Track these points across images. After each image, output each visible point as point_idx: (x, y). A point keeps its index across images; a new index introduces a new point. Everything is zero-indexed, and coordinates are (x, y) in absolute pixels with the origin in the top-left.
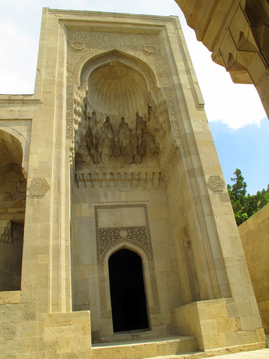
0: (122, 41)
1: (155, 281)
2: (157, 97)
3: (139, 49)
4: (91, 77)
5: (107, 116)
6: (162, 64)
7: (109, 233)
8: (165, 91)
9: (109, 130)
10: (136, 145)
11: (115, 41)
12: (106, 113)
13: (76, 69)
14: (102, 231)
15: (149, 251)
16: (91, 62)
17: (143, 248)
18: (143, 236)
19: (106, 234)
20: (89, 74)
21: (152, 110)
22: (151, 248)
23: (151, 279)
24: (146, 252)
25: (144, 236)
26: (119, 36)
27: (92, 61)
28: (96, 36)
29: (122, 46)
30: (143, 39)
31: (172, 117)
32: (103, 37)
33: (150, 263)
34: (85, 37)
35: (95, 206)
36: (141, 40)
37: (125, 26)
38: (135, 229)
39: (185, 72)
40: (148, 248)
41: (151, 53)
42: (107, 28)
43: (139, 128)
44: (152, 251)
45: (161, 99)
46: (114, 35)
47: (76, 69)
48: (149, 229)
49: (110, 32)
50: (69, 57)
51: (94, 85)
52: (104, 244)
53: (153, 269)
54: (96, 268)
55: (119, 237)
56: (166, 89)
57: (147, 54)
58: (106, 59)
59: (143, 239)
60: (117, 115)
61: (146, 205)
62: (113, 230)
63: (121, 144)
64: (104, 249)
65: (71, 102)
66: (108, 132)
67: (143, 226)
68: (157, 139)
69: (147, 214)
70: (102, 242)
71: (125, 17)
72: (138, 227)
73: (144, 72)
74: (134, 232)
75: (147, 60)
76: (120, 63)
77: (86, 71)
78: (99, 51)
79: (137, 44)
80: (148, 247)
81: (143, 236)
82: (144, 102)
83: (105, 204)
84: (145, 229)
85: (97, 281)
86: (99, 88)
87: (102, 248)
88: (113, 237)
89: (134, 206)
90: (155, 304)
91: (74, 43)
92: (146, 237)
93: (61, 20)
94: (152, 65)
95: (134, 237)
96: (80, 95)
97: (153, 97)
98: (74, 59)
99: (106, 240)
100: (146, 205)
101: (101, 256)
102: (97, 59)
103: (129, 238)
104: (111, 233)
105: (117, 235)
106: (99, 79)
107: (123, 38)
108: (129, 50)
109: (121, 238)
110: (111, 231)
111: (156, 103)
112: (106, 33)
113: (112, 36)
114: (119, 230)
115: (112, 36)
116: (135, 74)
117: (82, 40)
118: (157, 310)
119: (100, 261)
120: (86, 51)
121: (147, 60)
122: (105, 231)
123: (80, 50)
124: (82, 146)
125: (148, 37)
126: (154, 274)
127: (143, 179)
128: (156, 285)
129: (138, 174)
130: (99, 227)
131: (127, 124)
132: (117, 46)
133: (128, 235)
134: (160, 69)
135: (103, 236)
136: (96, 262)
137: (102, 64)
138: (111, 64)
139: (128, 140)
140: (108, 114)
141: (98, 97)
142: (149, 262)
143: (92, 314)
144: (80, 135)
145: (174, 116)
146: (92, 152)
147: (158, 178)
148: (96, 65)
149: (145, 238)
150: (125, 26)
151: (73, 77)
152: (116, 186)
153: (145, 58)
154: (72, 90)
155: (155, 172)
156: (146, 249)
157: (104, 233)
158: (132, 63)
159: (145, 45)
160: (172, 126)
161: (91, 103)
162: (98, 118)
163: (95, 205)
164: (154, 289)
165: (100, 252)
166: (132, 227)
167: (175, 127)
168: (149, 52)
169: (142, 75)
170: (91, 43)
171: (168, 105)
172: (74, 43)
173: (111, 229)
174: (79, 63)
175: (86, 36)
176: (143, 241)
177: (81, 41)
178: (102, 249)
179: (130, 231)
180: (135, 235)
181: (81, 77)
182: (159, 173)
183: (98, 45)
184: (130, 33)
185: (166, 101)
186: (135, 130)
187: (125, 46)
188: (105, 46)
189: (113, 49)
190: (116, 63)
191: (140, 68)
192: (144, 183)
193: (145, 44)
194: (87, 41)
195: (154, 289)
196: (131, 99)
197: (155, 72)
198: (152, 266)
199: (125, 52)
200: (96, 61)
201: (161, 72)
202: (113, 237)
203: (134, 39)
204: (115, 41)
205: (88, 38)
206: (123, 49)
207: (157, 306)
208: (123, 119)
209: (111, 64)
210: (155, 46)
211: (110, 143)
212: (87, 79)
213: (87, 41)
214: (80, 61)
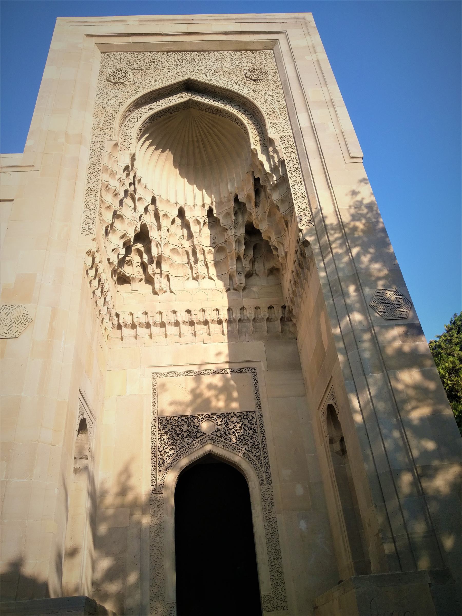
1: (275, 530)
2: (269, 158)
3: (234, 76)
6: (279, 96)
8: (283, 142)
11: (189, 65)
13: (111, 115)
15: (261, 463)
17: (249, 458)
18: (248, 431)
19: (173, 428)
22: (266, 457)
23: (267, 527)
24: (255, 465)
25: (251, 432)
26: (197, 57)
31: (296, 187)
33: (264, 490)
36: (240, 59)
38: (232, 417)
40: (259, 458)
41: (257, 80)
44: (267, 463)
47: (111, 115)
48: (262, 416)
50: (100, 96)
52: (167, 450)
53: (271, 504)
55: (199, 435)
56: (286, 139)
59: (249, 438)
61: (255, 368)
62: (185, 420)
64: (166, 460)
65: (96, 170)
67: (250, 412)
70: (164, 445)
72: (238, 413)
74: (230, 423)
75: (249, 92)
78: (157, 83)
80: (258, 454)
81: (248, 431)
84: (253, 417)
88: (185, 435)
90: (275, 586)
91: (111, 72)
92: (255, 432)
94: (258, 100)
95: (229, 433)
98: (109, 98)
99: (171, 442)
103: (219, 435)
105: (195, 430)
107: (204, 60)
108: (215, 79)
109: (202, 435)
110: (183, 423)
111: (267, 168)
113: (184, 58)
114: (199, 421)
118: (279, 603)
120: (134, 84)
122: (170, 421)
123: (122, 83)
125: (253, 55)
126: (273, 515)
128: (277, 541)
133: (218, 430)
142: (262, 487)
145: (299, 185)
149: (254, 436)
153: (246, 89)
156: (254, 458)
157: (168, 426)
160: (296, 204)
164: (273, 551)
166: (227, 413)
167: (300, 205)
168: (253, 78)
171: (289, 167)
173: (182, 418)
174: (118, 104)
175: (135, 61)
176: (248, 443)
178: (161, 461)
179: (221, 421)
180: (233, 430)
182: (282, 307)
183: (156, 74)
185: (284, 160)
193: (247, 66)
195: (273, 551)
198: (268, 496)
199: (207, 82)
202: (185, 435)
204: (189, 65)
206: (204, 77)
207: (280, 590)
214: (120, 101)
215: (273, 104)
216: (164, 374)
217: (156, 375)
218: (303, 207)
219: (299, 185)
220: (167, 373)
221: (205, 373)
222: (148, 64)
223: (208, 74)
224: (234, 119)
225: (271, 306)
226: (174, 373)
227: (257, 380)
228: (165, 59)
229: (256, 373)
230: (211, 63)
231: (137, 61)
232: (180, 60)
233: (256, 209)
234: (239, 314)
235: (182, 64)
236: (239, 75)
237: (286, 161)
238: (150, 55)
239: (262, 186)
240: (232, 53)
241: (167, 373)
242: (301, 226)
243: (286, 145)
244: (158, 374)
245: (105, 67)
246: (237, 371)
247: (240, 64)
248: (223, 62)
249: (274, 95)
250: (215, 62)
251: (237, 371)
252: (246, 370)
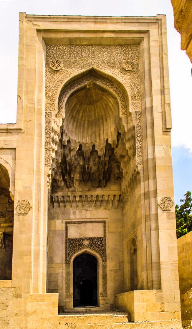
0: (101, 56)
2: (127, 123)
3: (116, 67)
4: (68, 103)
7: (75, 242)
9: (81, 157)
10: (103, 170)
11: (93, 57)
14: (70, 240)
16: (68, 85)
20: (66, 99)
21: (121, 137)
27: (69, 84)
28: (74, 51)
29: (100, 63)
30: (123, 53)
32: (82, 52)
34: (63, 53)
36: (121, 53)
37: (106, 35)
39: (159, 92)
42: (87, 39)
43: (107, 155)
45: (131, 124)
46: (93, 49)
49: (89, 45)
54: (64, 266)
57: (124, 72)
58: (83, 81)
60: (89, 142)
63: (91, 170)
66: (80, 159)
68: (122, 166)
71: (106, 22)
73: (119, 95)
76: (96, 85)
77: (64, 96)
79: (116, 60)
82: (115, 128)
85: (64, 275)
87: (69, 253)
89: (96, 222)
93: (39, 31)
94: (127, 86)
96: (57, 123)
97: (124, 123)
101: (68, 258)
102: (74, 81)
104: (77, 242)
107: (101, 53)
112: (85, 47)
115: (90, 51)
116: (109, 97)
117: (60, 58)
119: (67, 261)
121: (123, 79)
125: (128, 50)
127: (105, 201)
130: (68, 237)
132: (95, 64)
134: (135, 90)
135: (71, 244)
136: (64, 262)
137: (79, 86)
138: (88, 87)
139: (97, 167)
141: (73, 125)
143: (59, 296)
148: (73, 88)
150: (106, 35)
151: (51, 103)
152: (83, 206)
154: (50, 117)
158: (108, 84)
159: (123, 61)
162: (72, 145)
165: (68, 255)
169: (116, 98)
170: (68, 60)
172: (52, 62)
177: (59, 59)
181: (58, 104)
184: (109, 46)
186: (103, 157)
187: (103, 63)
188: (83, 64)
189: (91, 68)
191: (115, 90)
192: (106, 203)
193: (124, 59)
194: (65, 59)
196: (103, 125)
197: (129, 93)
200: (73, 84)
201: (135, 94)
203: (113, 53)
205: (66, 54)
206: (101, 67)
209: (88, 87)
210: (134, 61)
211: (81, 170)
212: (64, 106)
213: (65, 59)
215: (134, 89)
218: (140, 155)
219: (140, 142)
222: (71, 56)
223: (103, 65)
224: (113, 96)
228: (80, 51)
230: (105, 55)
231: (66, 52)
232: (89, 53)
235: (89, 56)
236: (119, 66)
237: (136, 127)
238: (73, 47)
240: (117, 48)
243: (137, 118)
245: (48, 57)
247: (120, 57)
248: (111, 55)
249: (135, 82)
250: (107, 55)
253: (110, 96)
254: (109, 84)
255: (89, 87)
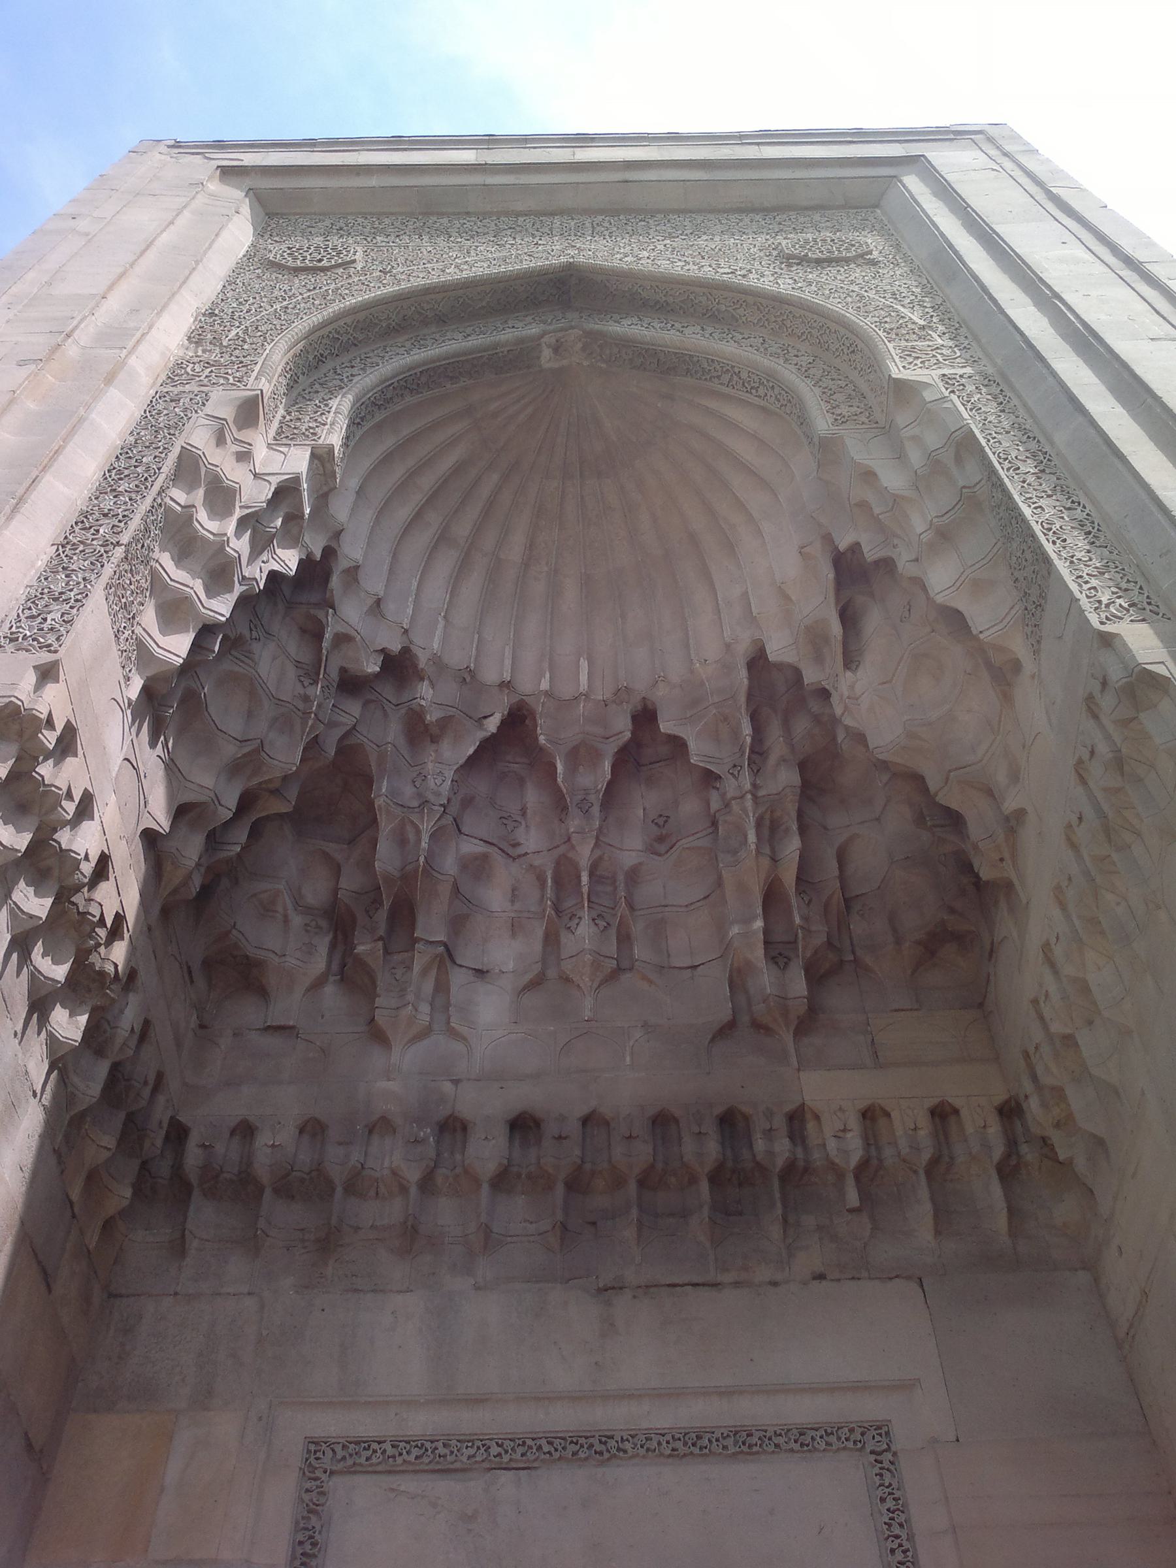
5: (515, 699)
12: (507, 677)
35: (315, 1447)
51: (415, 499)
61: (882, 1429)
69: (911, 1538)
83: (420, 1423)
86: (462, 530)
100: (882, 1429)
106: (458, 470)
124: (280, 909)
129: (779, 1122)
131: (678, 745)
138: (547, 358)
140: (526, 685)
144: (235, 768)
146: (360, 949)
147: (998, 1152)
155: (957, 1103)
161: (374, 583)
163: (319, 1433)
190: (584, 349)
208: (645, 717)
216: (375, 1446)
217: (329, 1453)
220: (387, 1446)
221: (603, 1448)
225: (942, 1103)
226: (428, 1445)
227: (897, 1494)
229: (889, 1456)
233: (849, 674)
234: (786, 1141)
239: (877, 563)
241: (387, 1446)
242: (1102, 623)
244: (338, 1448)
246: (780, 1440)
251: (780, 1440)
252: (833, 1439)
253: (725, 390)
254: (703, 329)
255: (555, 365)
